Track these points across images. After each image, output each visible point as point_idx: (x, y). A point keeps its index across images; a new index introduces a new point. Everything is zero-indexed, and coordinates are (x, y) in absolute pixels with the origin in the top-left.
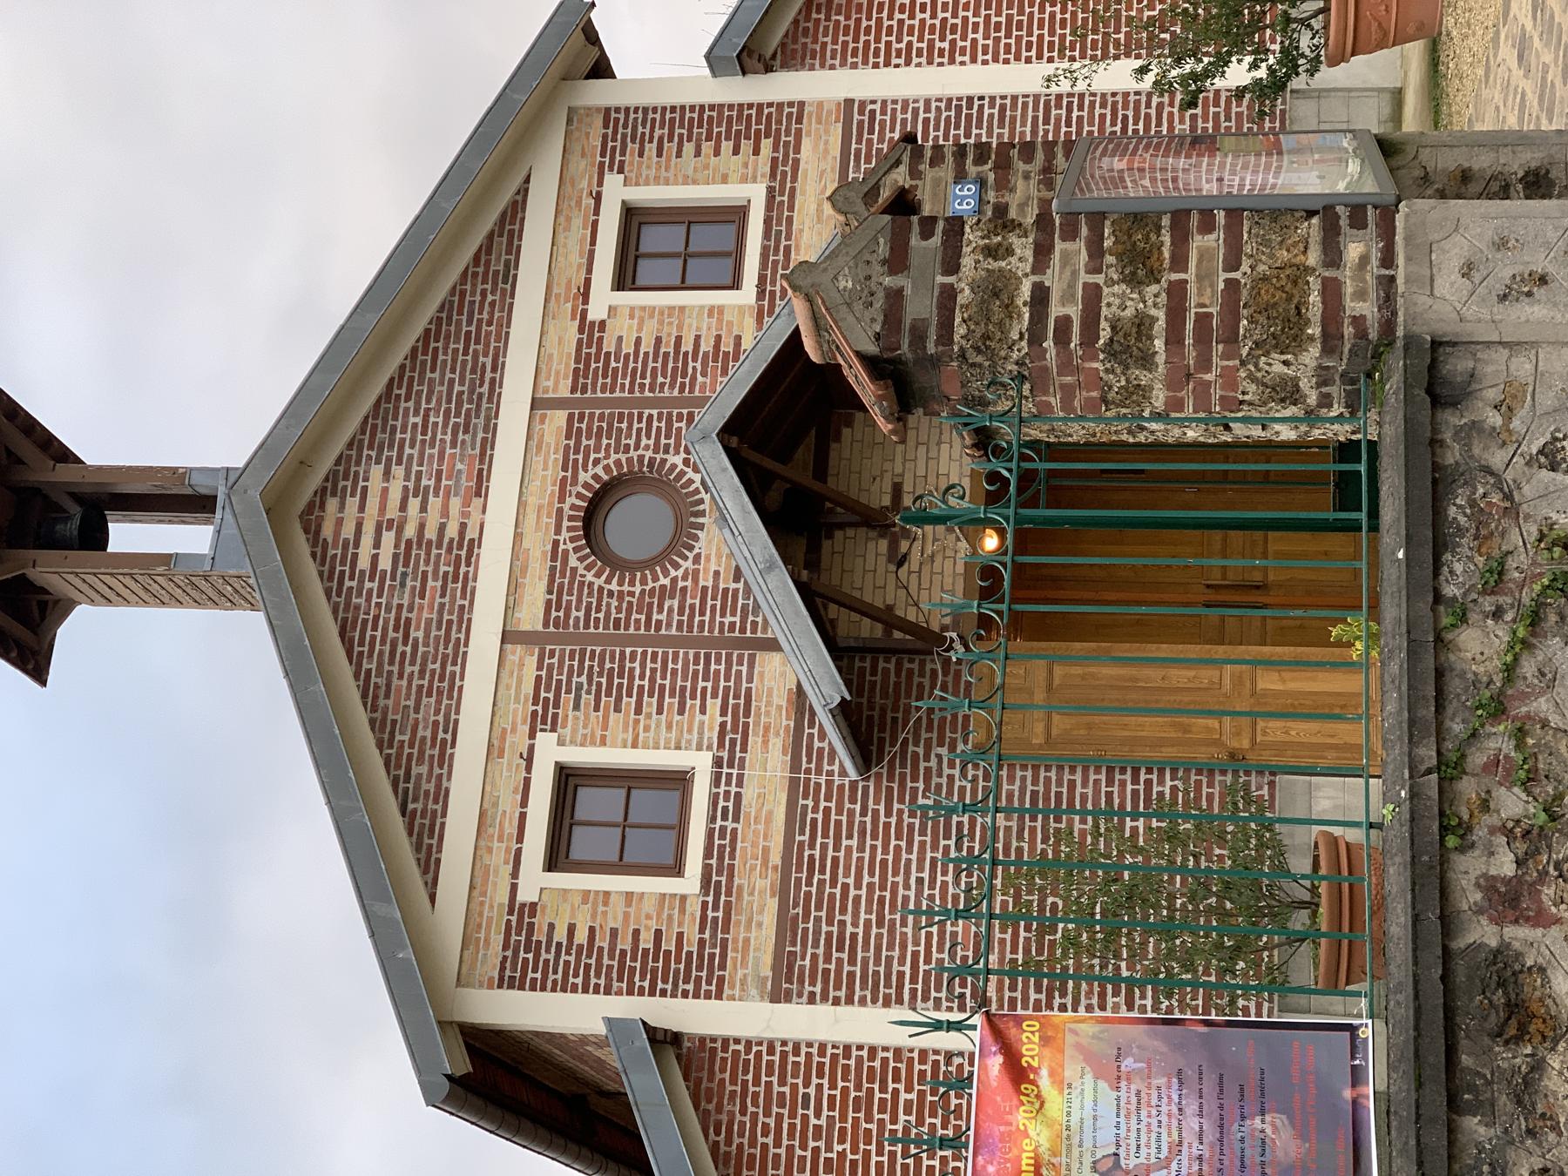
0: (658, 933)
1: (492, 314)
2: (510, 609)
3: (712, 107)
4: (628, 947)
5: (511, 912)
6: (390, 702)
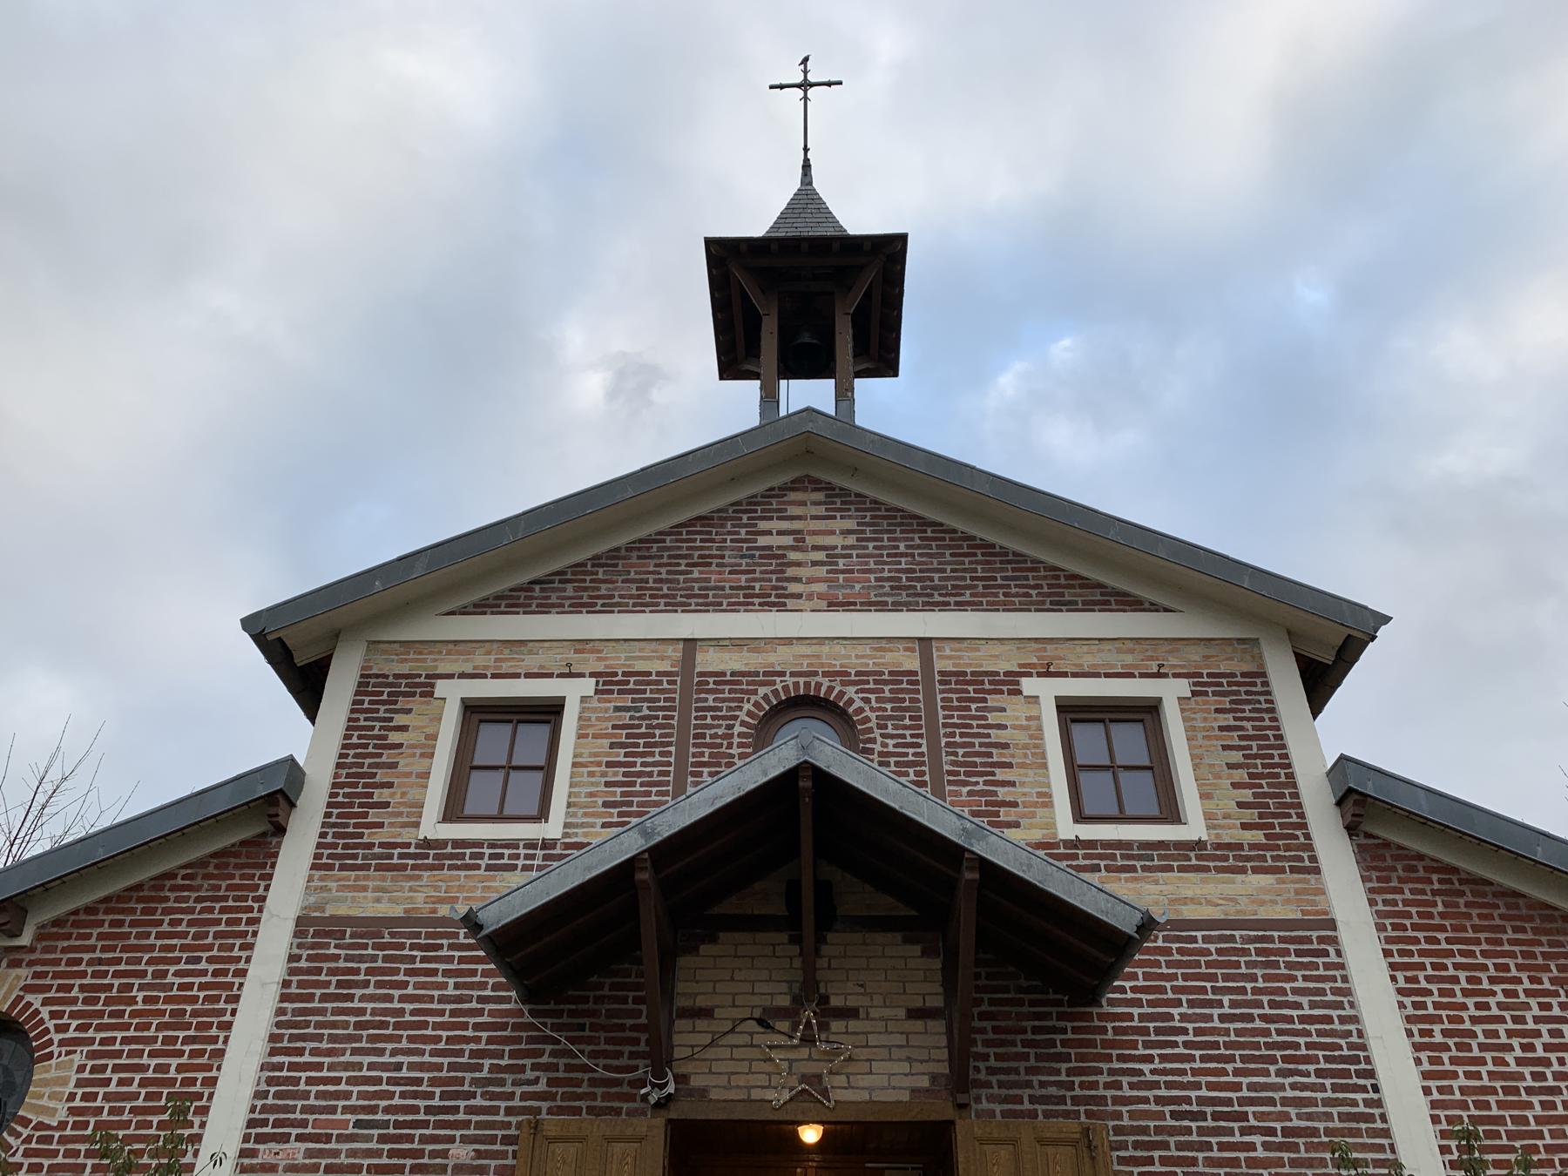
0: (387, 805)
1: (1017, 595)
2: (717, 642)
3: (1291, 776)
4: (377, 779)
5: (427, 676)
6: (634, 561)
